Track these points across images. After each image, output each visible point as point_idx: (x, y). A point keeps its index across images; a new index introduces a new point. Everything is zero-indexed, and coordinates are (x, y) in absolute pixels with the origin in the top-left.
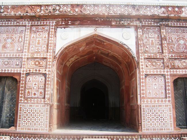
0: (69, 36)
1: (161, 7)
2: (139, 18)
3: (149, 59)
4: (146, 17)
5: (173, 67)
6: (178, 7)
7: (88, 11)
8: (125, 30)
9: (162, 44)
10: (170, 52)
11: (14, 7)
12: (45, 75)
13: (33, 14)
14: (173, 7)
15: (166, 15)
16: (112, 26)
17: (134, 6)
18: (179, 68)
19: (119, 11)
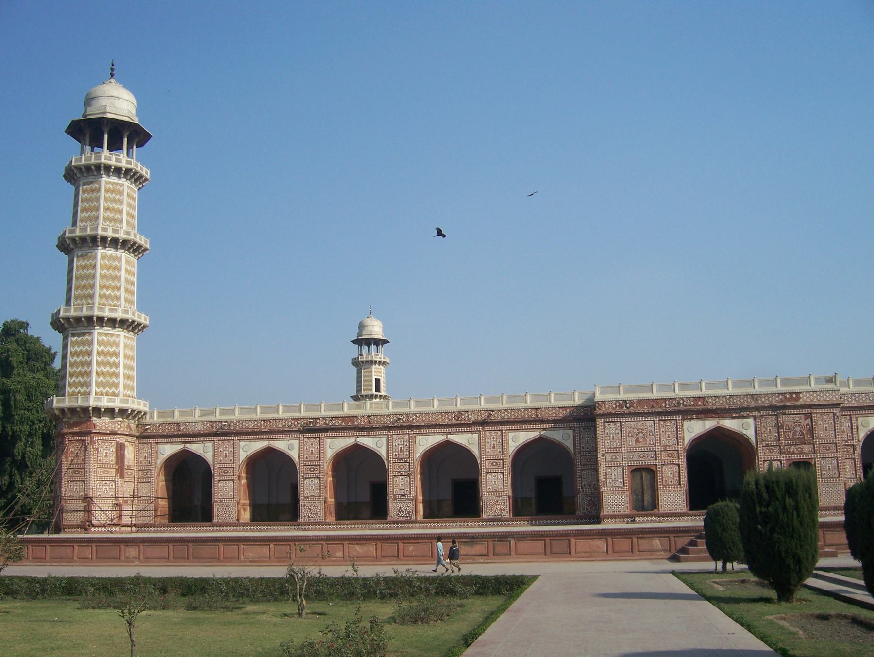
0: (695, 428)
1: (780, 394)
2: (757, 409)
3: (767, 445)
4: (763, 408)
5: (789, 453)
6: (795, 393)
8: (745, 420)
9: (778, 432)
10: (786, 439)
11: (640, 401)
12: (678, 465)
13: (660, 410)
14: (791, 394)
15: (782, 404)
16: (734, 418)
17: (752, 395)
18: (794, 453)
19: (739, 403)
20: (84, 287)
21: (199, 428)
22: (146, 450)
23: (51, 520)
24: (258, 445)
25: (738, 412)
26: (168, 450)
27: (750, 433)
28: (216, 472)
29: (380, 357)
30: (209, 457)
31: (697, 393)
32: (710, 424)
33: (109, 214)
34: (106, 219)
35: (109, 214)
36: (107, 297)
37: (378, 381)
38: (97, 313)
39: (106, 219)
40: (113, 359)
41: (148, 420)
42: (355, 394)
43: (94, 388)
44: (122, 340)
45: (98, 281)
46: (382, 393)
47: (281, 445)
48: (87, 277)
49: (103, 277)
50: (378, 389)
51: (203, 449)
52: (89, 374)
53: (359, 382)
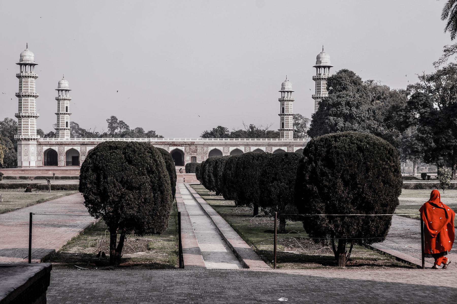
7: (175, 143)
20: (26, 107)
21: (54, 143)
22: (39, 148)
23: (16, 166)
24: (70, 148)
25: (181, 145)
26: (45, 148)
27: (184, 150)
28: (58, 154)
29: (68, 97)
30: (57, 150)
31: (173, 141)
32: (175, 148)
33: (31, 88)
34: (30, 90)
35: (31, 88)
36: (31, 110)
37: (67, 107)
38: (30, 115)
39: (30, 90)
40: (33, 126)
41: (40, 141)
42: (57, 112)
43: (29, 134)
44: (35, 121)
45: (29, 106)
46: (68, 112)
47: (75, 148)
48: (26, 105)
49: (30, 105)
50: (67, 111)
51: (56, 148)
52: (28, 130)
53: (59, 107)
